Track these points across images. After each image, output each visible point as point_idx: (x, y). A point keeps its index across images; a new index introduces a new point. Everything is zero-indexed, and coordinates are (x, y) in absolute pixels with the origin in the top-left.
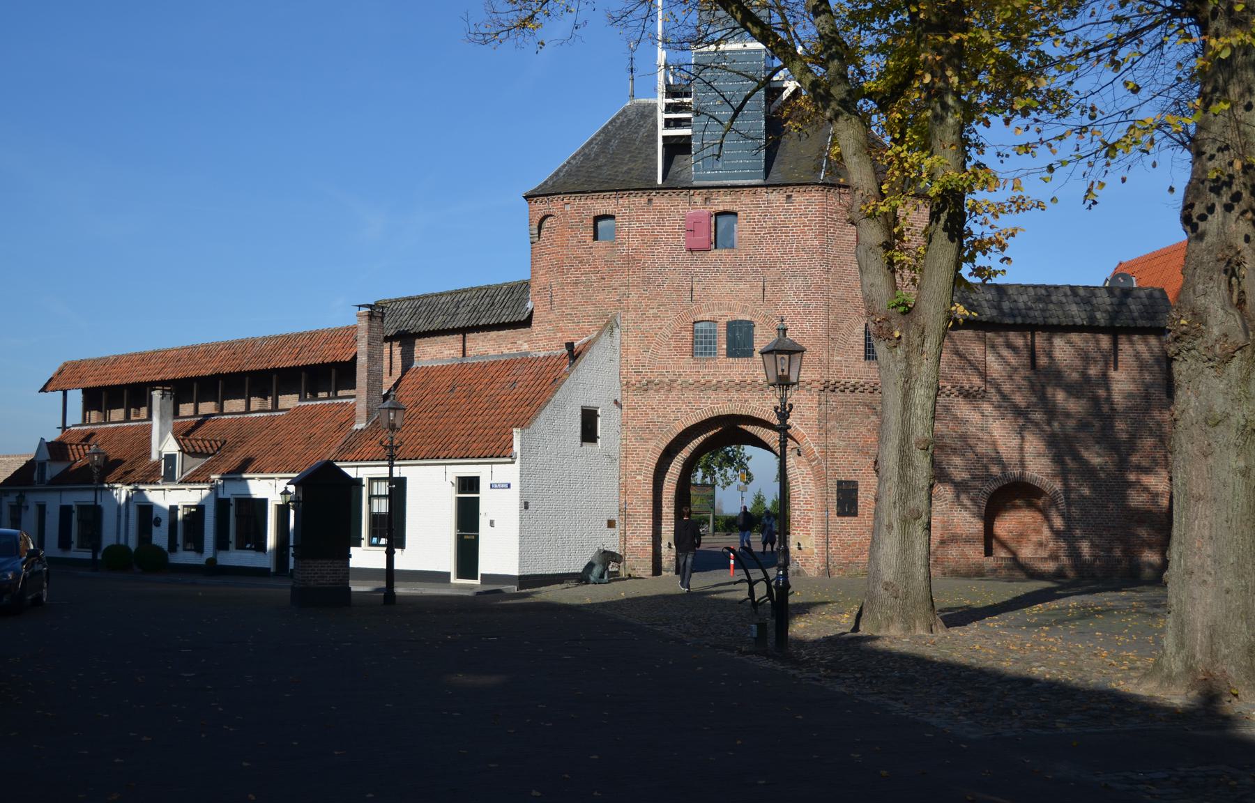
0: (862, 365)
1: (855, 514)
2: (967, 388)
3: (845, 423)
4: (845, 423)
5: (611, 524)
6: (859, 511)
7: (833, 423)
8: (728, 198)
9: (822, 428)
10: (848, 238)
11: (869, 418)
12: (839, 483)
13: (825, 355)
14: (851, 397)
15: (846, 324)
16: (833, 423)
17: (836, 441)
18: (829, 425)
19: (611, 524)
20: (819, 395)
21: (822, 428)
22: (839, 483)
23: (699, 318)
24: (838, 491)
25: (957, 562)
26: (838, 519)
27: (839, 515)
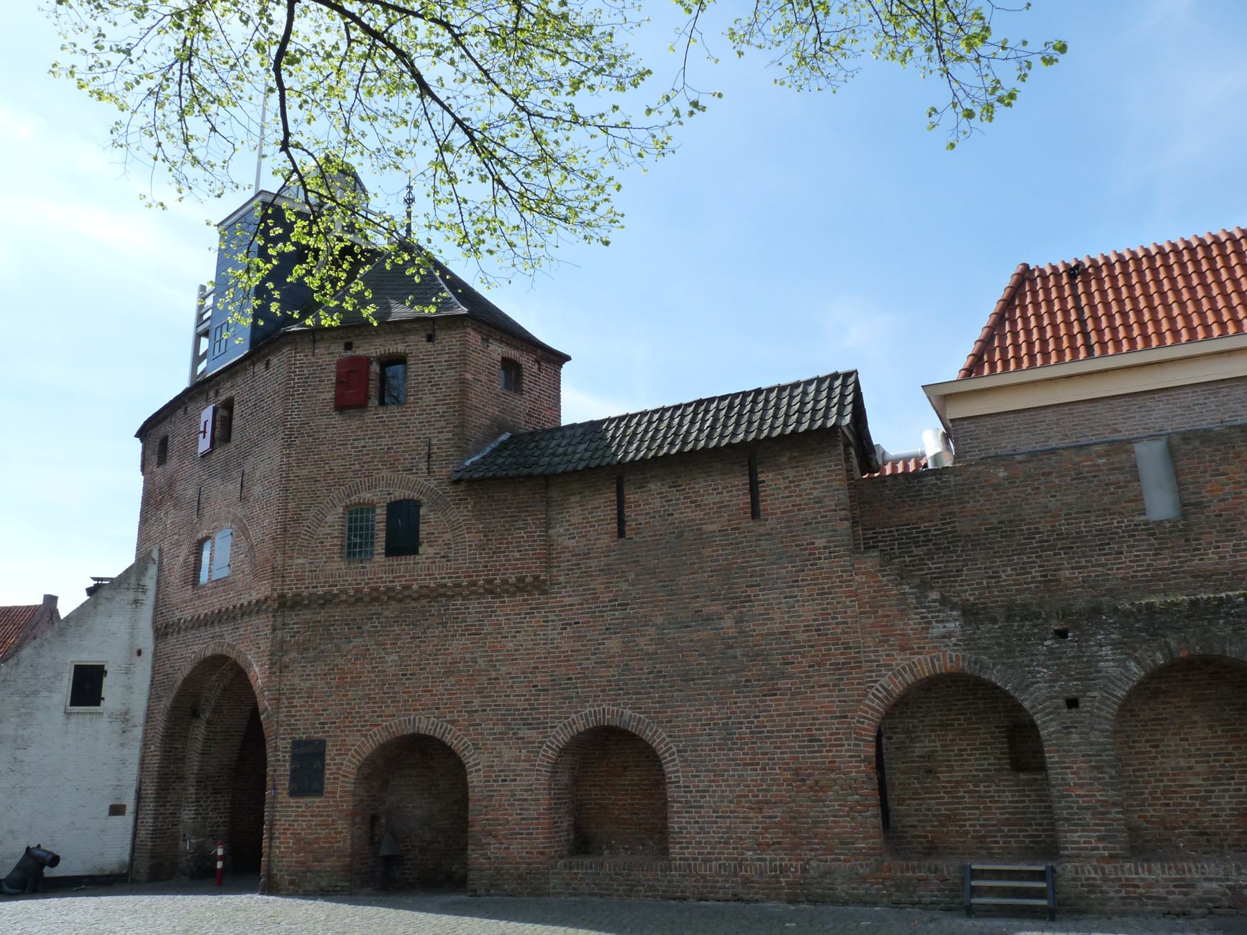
0: (338, 565)
1: (319, 792)
2: (512, 580)
3: (312, 654)
4: (312, 654)
5: (116, 810)
6: (328, 787)
7: (293, 655)
8: (229, 385)
9: (275, 663)
10: (322, 396)
11: (350, 642)
12: (296, 744)
13: (279, 559)
14: (322, 615)
15: (313, 512)
16: (293, 655)
17: (296, 681)
18: (286, 659)
19: (116, 810)
20: (274, 616)
21: (275, 663)
22: (296, 744)
23: (200, 536)
24: (294, 758)
25: (496, 869)
26: (292, 801)
27: (293, 794)
